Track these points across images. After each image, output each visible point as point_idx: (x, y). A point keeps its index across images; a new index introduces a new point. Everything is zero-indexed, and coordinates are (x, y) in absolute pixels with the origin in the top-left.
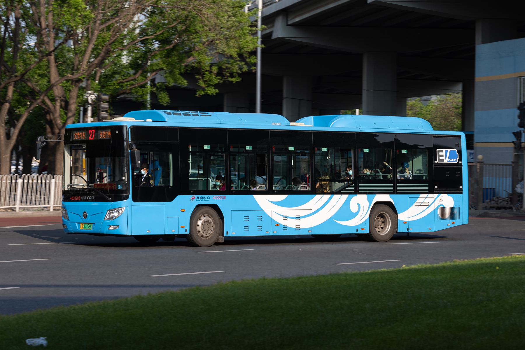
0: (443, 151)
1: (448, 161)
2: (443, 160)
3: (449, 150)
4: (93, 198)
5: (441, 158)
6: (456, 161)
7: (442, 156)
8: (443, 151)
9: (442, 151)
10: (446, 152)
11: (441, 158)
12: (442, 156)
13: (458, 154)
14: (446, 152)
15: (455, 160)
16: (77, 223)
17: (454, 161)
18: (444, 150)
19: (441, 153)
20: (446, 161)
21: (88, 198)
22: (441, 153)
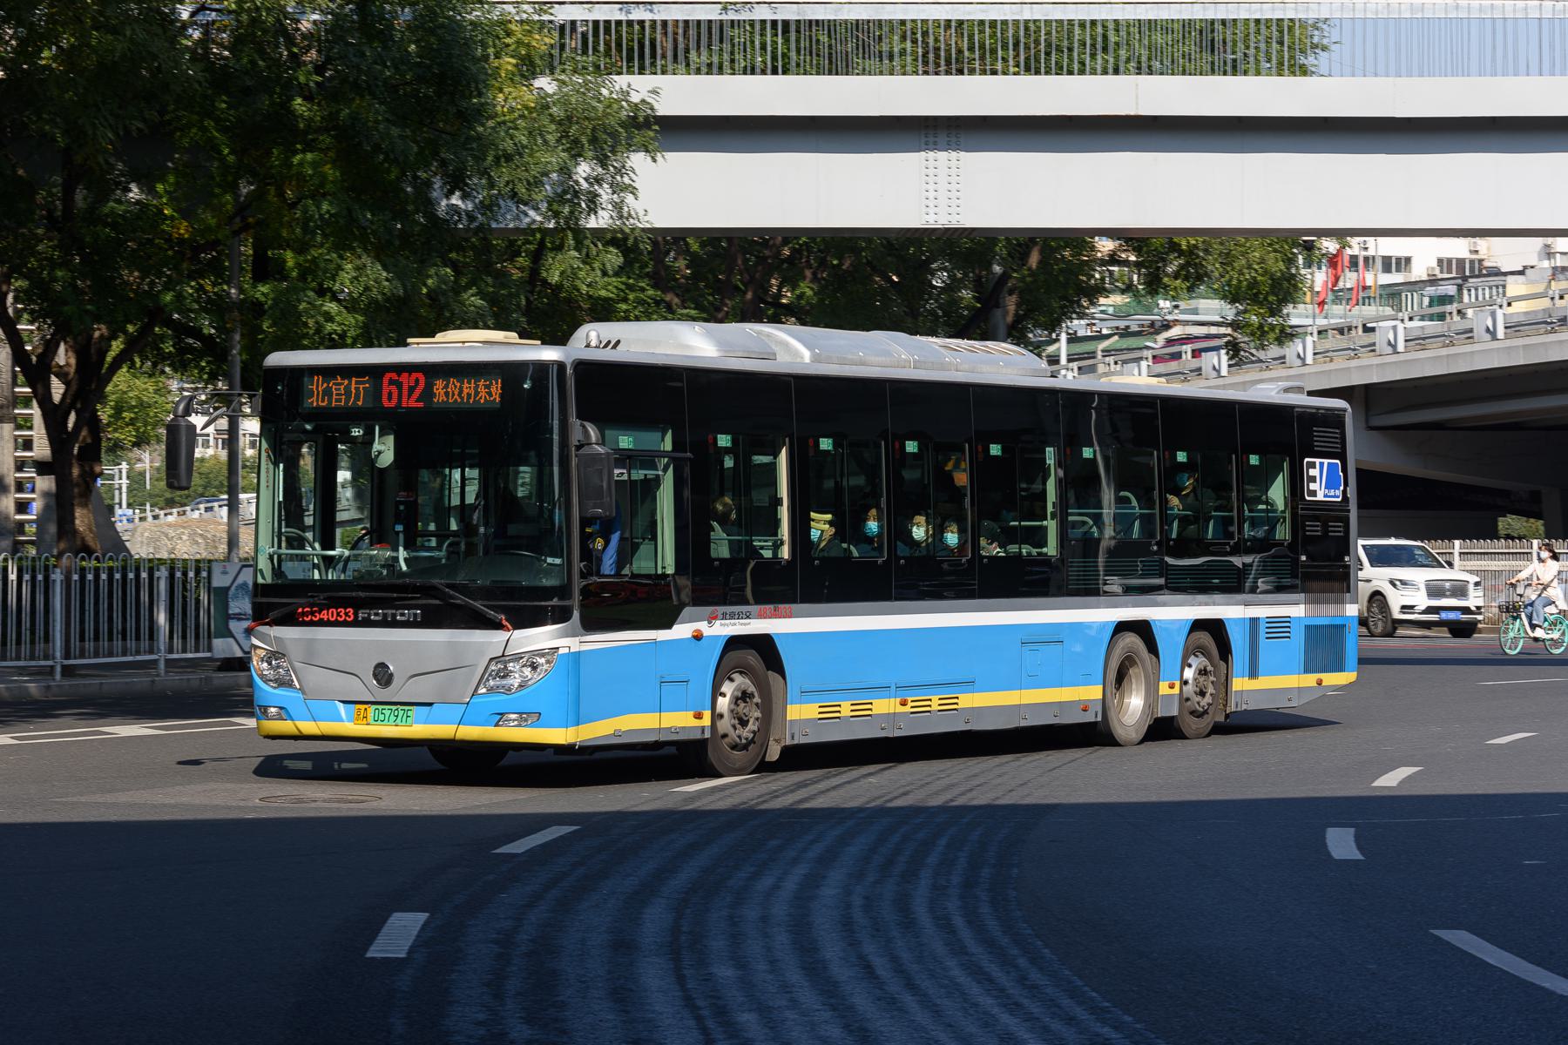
1: (1325, 496)
2: (1314, 493)
3: (1326, 461)
4: (415, 615)
5: (1313, 486)
6: (1336, 496)
7: (1313, 479)
9: (1313, 465)
10: (1322, 465)
11: (1313, 486)
12: (1313, 479)
14: (1322, 465)
16: (344, 702)
17: (1335, 496)
18: (1318, 461)
19: (1312, 472)
20: (1320, 497)
21: (394, 616)
22: (1312, 472)
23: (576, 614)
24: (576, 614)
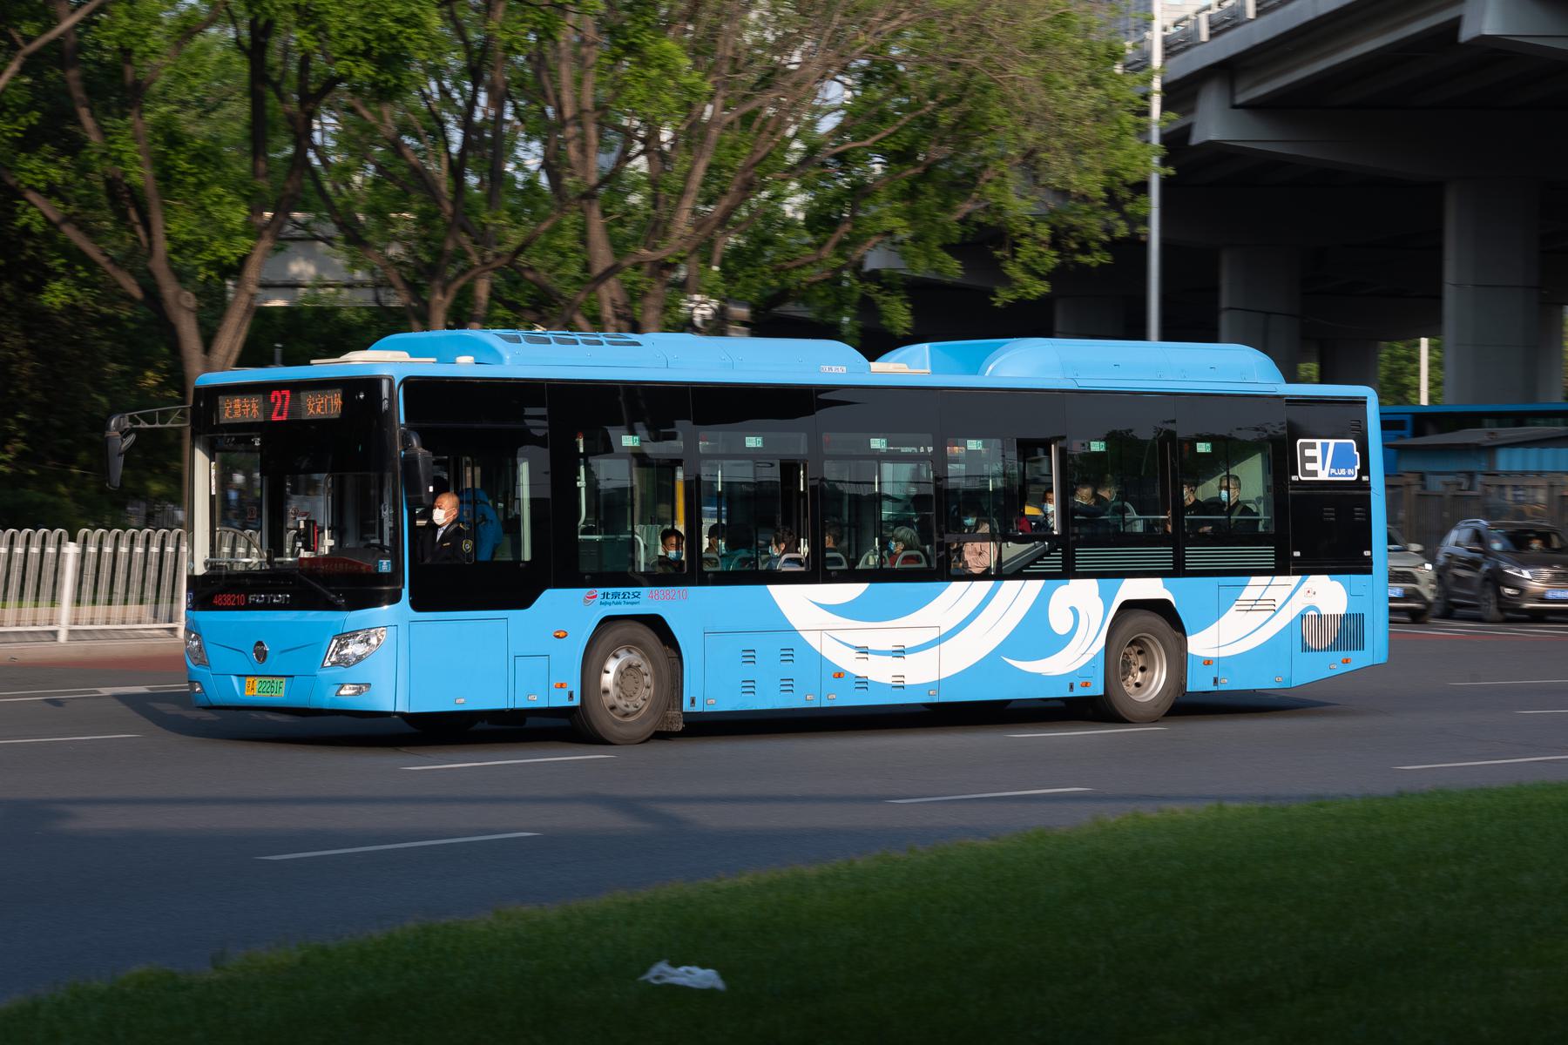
0: (1315, 443)
1: (1330, 476)
2: (1315, 473)
3: (1332, 442)
5: (1309, 466)
7: (1313, 460)
8: (1315, 443)
9: (1313, 446)
10: (1325, 448)
11: (1309, 466)
12: (1313, 460)
13: (1358, 454)
14: (1325, 448)
15: (1350, 471)
17: (1347, 475)
18: (1319, 442)
19: (1308, 453)
20: (1323, 476)
22: (1308, 453)
23: (405, 592)
24: (405, 592)
